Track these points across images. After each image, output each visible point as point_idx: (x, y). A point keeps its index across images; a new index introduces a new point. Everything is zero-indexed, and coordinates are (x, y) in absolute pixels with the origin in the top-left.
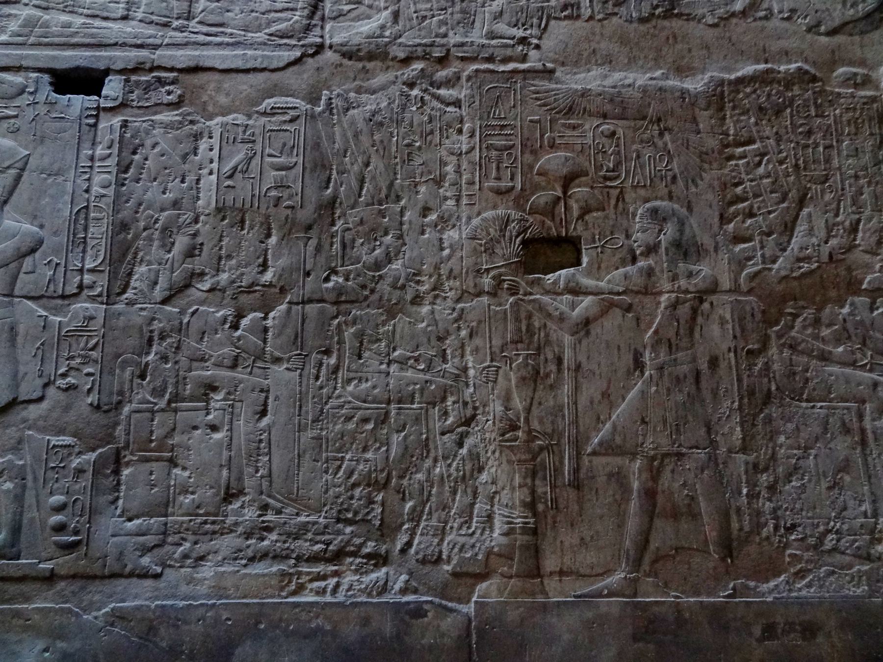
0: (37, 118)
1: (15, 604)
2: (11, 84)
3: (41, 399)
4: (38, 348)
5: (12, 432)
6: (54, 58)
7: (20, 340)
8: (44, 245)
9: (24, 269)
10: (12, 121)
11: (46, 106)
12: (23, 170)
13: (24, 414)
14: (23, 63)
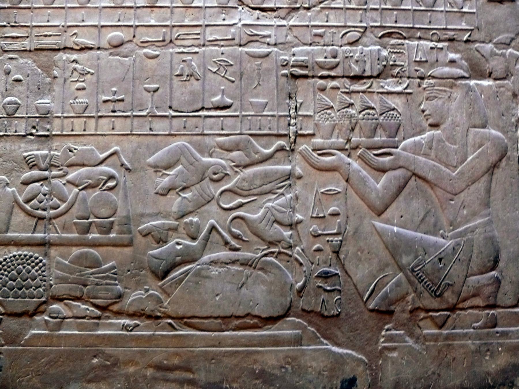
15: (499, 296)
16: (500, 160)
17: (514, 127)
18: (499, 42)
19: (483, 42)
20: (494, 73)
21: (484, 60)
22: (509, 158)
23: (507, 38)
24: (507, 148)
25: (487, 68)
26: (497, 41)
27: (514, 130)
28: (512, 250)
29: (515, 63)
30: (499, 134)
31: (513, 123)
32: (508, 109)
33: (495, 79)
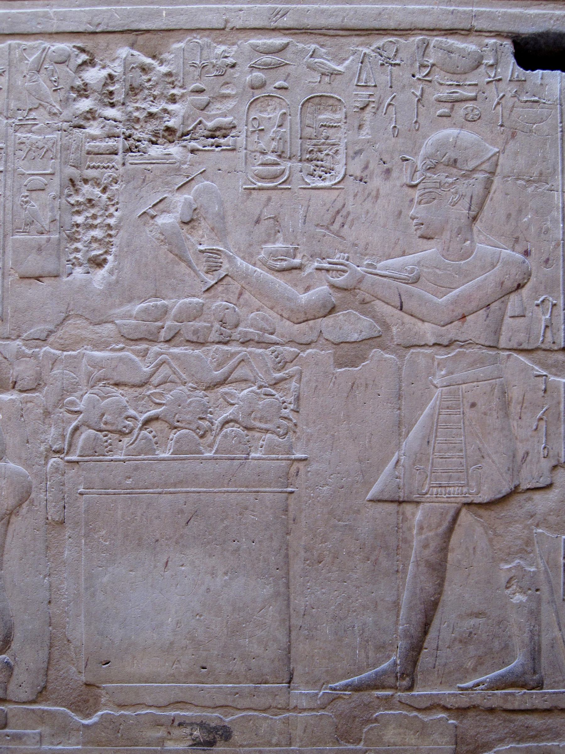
0: (503, 101)
1: (543, 741)
2: (464, 54)
3: (549, 486)
4: (541, 419)
5: (517, 529)
6: (515, 17)
7: (514, 409)
8: (533, 279)
9: (509, 313)
10: (470, 104)
11: (513, 84)
12: (493, 173)
13: (528, 506)
14: (474, 23)
15: (12, 687)
16: (20, 505)
17: (43, 458)
18: (31, 337)
19: (8, 338)
20: (19, 382)
21: (7, 363)
22: (32, 503)
23: (42, 331)
24: (31, 488)
25: (10, 375)
26: (26, 337)
27: (43, 462)
28: (30, 627)
29: (50, 366)
30: (21, 468)
31: (41, 453)
32: (35, 432)
33: (21, 391)
